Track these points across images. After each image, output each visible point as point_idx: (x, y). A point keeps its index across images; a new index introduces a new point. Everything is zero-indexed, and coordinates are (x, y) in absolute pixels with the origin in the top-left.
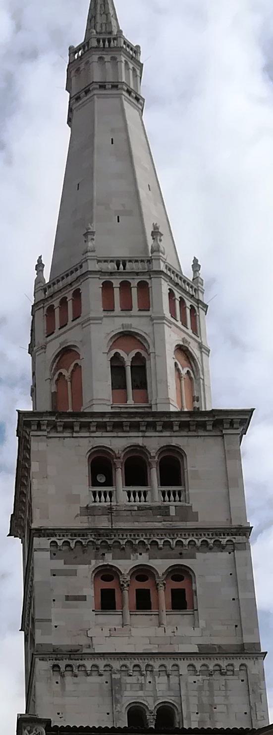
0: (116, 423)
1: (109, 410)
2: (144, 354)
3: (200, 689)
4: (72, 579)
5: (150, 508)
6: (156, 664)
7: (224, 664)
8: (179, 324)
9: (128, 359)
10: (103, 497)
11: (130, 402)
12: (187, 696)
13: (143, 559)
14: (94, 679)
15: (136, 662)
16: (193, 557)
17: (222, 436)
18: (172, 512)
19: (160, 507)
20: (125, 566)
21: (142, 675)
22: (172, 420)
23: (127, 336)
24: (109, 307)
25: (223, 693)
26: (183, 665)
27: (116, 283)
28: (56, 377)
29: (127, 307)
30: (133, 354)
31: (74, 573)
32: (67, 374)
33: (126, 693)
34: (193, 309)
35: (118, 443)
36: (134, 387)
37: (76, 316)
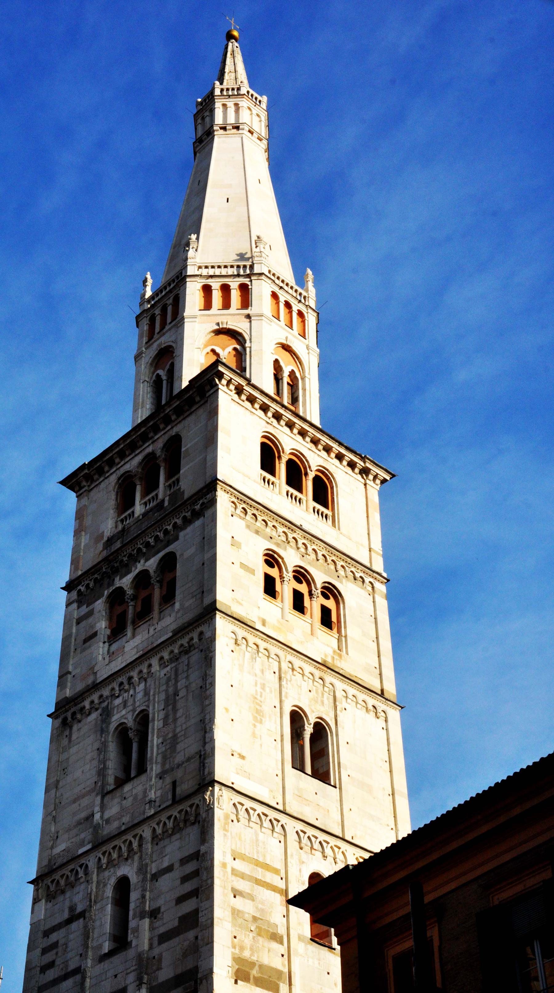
3: (169, 680)
4: (91, 620)
5: (151, 510)
6: (134, 674)
7: (184, 641)
12: (154, 695)
13: (140, 567)
14: (94, 716)
15: (120, 680)
16: (177, 538)
18: (166, 504)
19: (158, 505)
20: (125, 582)
21: (126, 691)
22: (167, 412)
25: (185, 675)
26: (155, 662)
29: (163, 326)
30: (168, 367)
31: (90, 613)
33: (115, 718)
35: (132, 464)
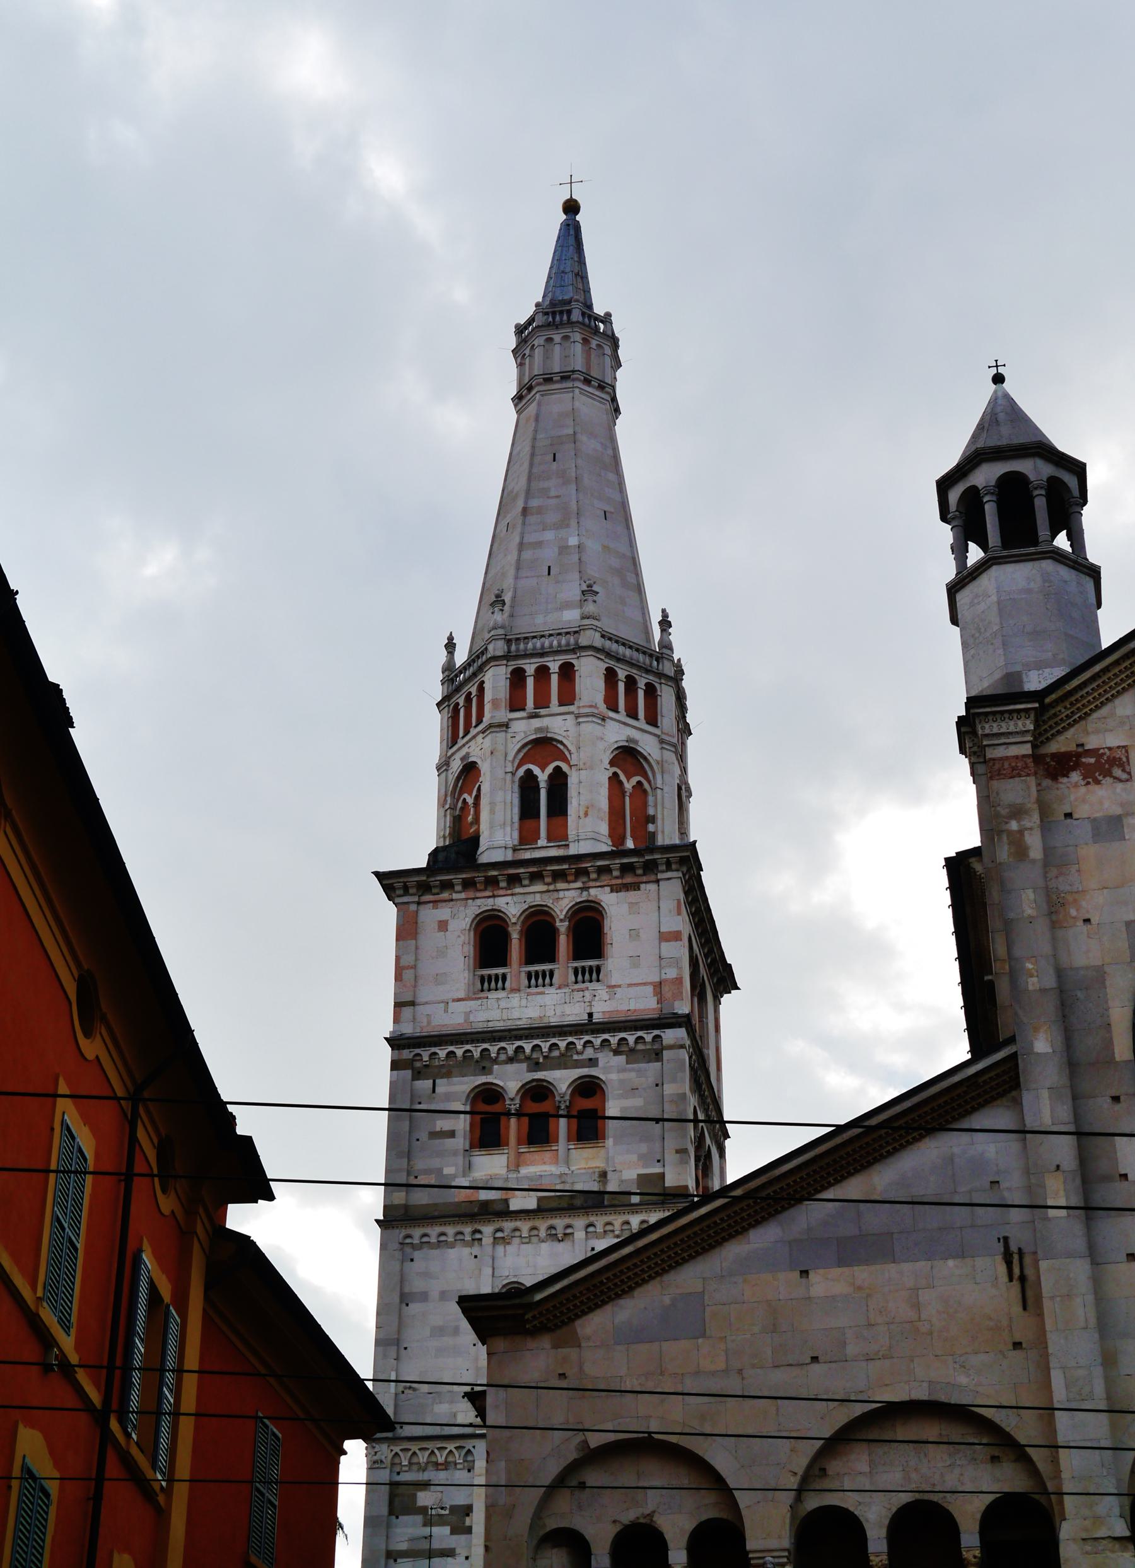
0: (510, 875)
1: (509, 856)
2: (564, 767)
8: (622, 716)
9: (543, 776)
10: (493, 984)
11: (542, 842)
17: (657, 881)
23: (543, 747)
24: (516, 704)
27: (530, 668)
28: (460, 804)
29: (542, 701)
30: (550, 769)
32: (470, 801)
34: (651, 691)
35: (513, 906)
36: (550, 814)
37: (479, 721)
